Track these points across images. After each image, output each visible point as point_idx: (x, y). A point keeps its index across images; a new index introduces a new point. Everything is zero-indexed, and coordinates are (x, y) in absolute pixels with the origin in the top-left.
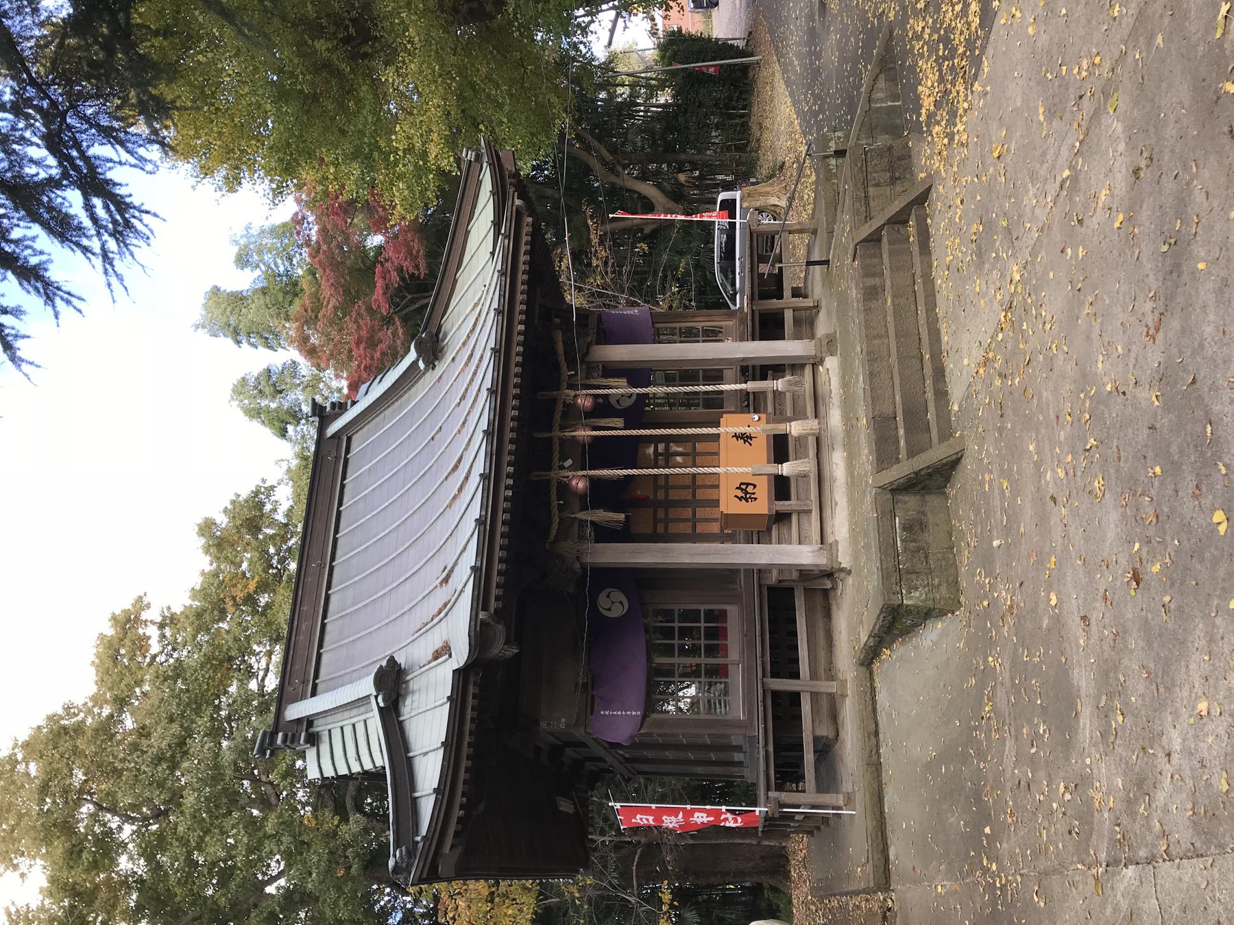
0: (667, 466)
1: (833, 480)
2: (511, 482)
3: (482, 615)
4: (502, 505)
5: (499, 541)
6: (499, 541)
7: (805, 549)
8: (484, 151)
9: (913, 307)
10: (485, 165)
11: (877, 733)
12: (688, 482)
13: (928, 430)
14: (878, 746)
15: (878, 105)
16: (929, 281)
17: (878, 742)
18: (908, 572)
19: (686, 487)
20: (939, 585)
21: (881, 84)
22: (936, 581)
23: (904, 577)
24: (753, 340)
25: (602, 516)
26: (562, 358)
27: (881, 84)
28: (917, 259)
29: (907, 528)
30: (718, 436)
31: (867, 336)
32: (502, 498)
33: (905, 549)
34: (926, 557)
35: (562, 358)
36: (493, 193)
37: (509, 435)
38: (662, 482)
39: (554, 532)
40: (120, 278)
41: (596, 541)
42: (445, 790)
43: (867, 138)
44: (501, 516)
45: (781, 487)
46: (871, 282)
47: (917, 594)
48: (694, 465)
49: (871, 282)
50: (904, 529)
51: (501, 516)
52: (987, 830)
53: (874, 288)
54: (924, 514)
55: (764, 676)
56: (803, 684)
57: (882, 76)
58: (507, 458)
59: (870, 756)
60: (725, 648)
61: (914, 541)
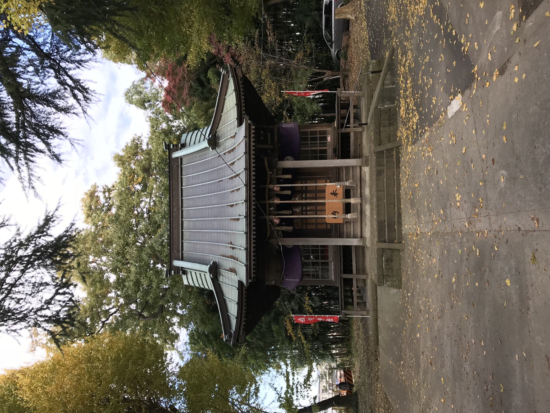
0: (306, 215)
1: (365, 215)
2: (255, 233)
3: (250, 281)
4: (253, 241)
5: (252, 254)
6: (252, 254)
7: (355, 240)
8: (229, 70)
9: (393, 184)
10: (230, 75)
11: (377, 300)
12: (314, 221)
13: (395, 231)
14: (377, 304)
15: (387, 87)
16: (399, 180)
17: (377, 302)
18: (386, 276)
19: (313, 224)
20: (396, 280)
21: (388, 77)
22: (395, 279)
23: (385, 277)
24: (338, 159)
25: (285, 228)
26: (267, 168)
27: (388, 77)
28: (395, 169)
29: (387, 261)
30: (325, 203)
31: (377, 191)
32: (252, 239)
33: (385, 268)
34: (392, 271)
35: (267, 168)
36: (235, 90)
37: (253, 215)
38: (304, 189)
39: (268, 234)
40: (90, 117)
41: (283, 237)
42: (239, 318)
43: (382, 103)
44: (253, 245)
45: (348, 208)
46: (379, 168)
47: (388, 283)
48: (316, 214)
49: (379, 168)
50: (386, 261)
51: (253, 245)
52: (402, 362)
53: (380, 170)
54: (392, 256)
55: (341, 273)
56: (354, 276)
57: (389, 72)
58: (253, 224)
59: (374, 307)
60: (328, 256)
61: (389, 265)
